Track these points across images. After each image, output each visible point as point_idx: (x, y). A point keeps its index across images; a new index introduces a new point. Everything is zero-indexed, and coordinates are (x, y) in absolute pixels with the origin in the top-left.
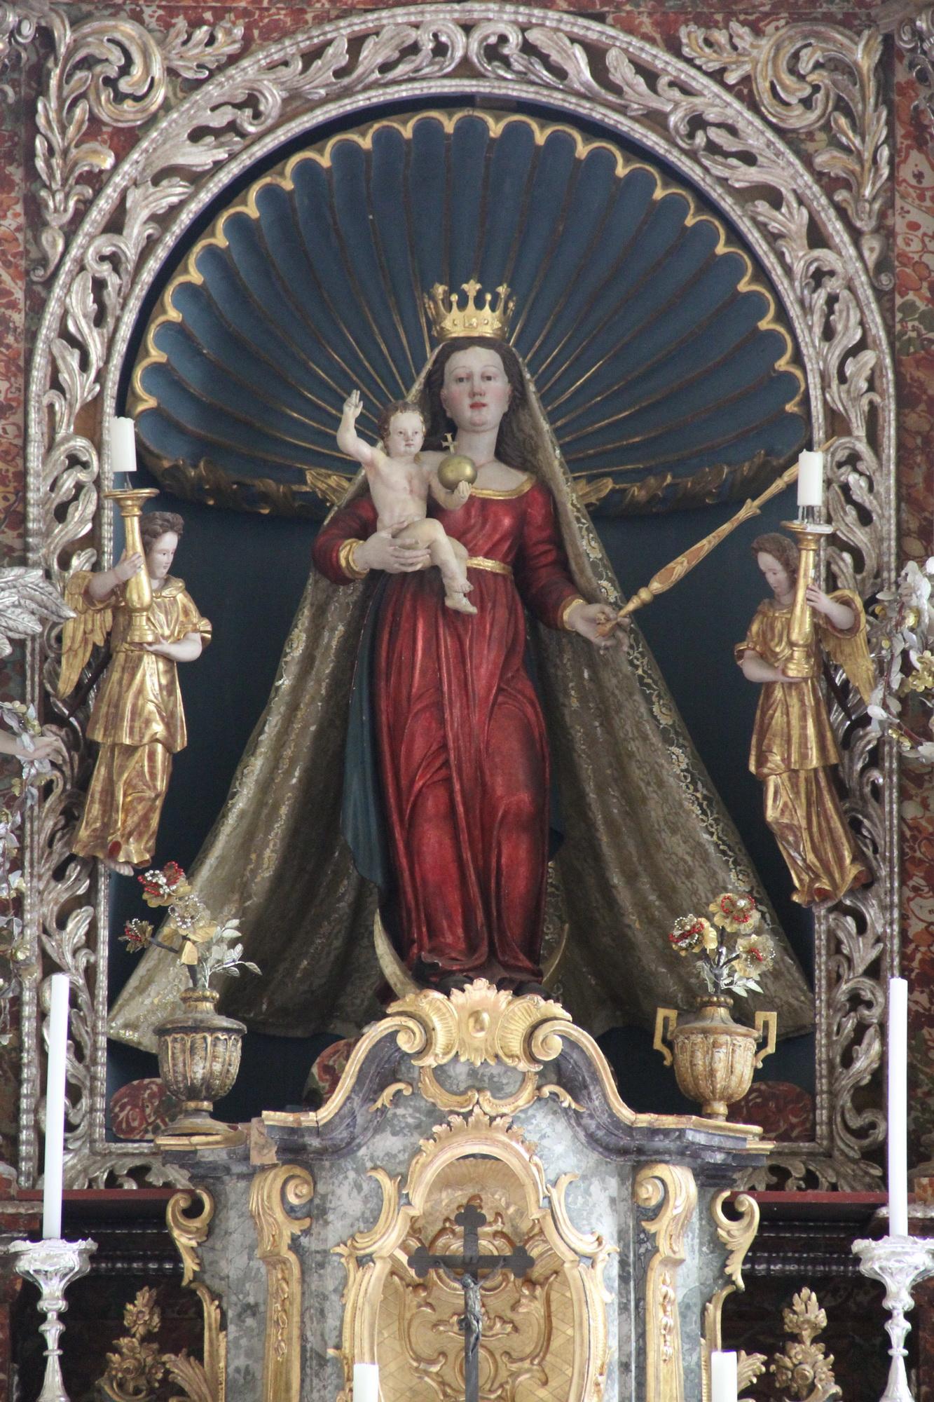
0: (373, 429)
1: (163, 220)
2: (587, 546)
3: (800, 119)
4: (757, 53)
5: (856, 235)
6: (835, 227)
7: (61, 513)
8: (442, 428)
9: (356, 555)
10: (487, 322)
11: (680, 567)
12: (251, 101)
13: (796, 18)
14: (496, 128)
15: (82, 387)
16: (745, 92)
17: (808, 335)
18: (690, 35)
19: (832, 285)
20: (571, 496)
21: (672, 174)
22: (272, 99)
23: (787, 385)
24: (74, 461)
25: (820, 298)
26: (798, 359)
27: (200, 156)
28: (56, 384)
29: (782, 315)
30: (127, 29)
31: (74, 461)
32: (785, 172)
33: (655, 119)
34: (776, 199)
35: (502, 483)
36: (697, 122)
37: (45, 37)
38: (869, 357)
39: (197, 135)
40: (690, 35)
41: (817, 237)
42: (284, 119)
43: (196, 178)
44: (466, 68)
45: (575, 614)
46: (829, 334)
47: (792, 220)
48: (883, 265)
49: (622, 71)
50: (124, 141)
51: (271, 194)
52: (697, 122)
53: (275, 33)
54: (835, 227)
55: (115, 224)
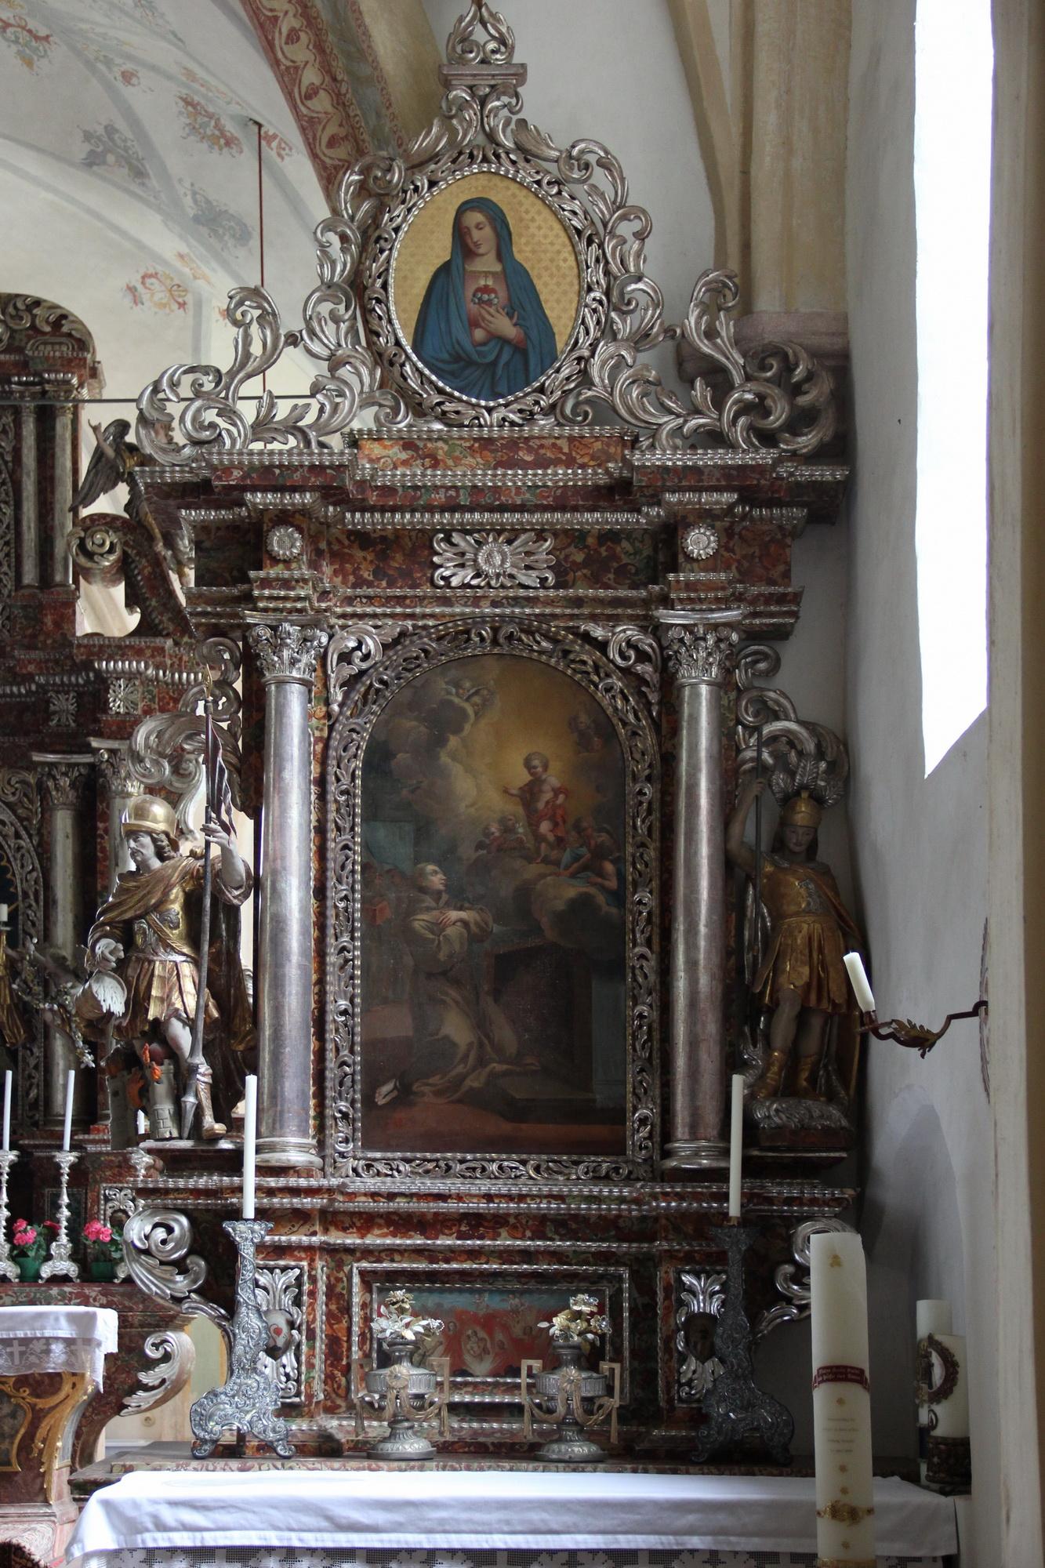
3: (12, 799)
5: (30, 836)
6: (23, 833)
13: (11, 767)
17: (16, 866)
19: (23, 851)
23: (11, 883)
25: (19, 856)
26: (14, 875)
29: (9, 861)
38: (35, 874)
41: (18, 836)
46: (22, 866)
47: (11, 831)
48: (40, 844)
54: (23, 833)
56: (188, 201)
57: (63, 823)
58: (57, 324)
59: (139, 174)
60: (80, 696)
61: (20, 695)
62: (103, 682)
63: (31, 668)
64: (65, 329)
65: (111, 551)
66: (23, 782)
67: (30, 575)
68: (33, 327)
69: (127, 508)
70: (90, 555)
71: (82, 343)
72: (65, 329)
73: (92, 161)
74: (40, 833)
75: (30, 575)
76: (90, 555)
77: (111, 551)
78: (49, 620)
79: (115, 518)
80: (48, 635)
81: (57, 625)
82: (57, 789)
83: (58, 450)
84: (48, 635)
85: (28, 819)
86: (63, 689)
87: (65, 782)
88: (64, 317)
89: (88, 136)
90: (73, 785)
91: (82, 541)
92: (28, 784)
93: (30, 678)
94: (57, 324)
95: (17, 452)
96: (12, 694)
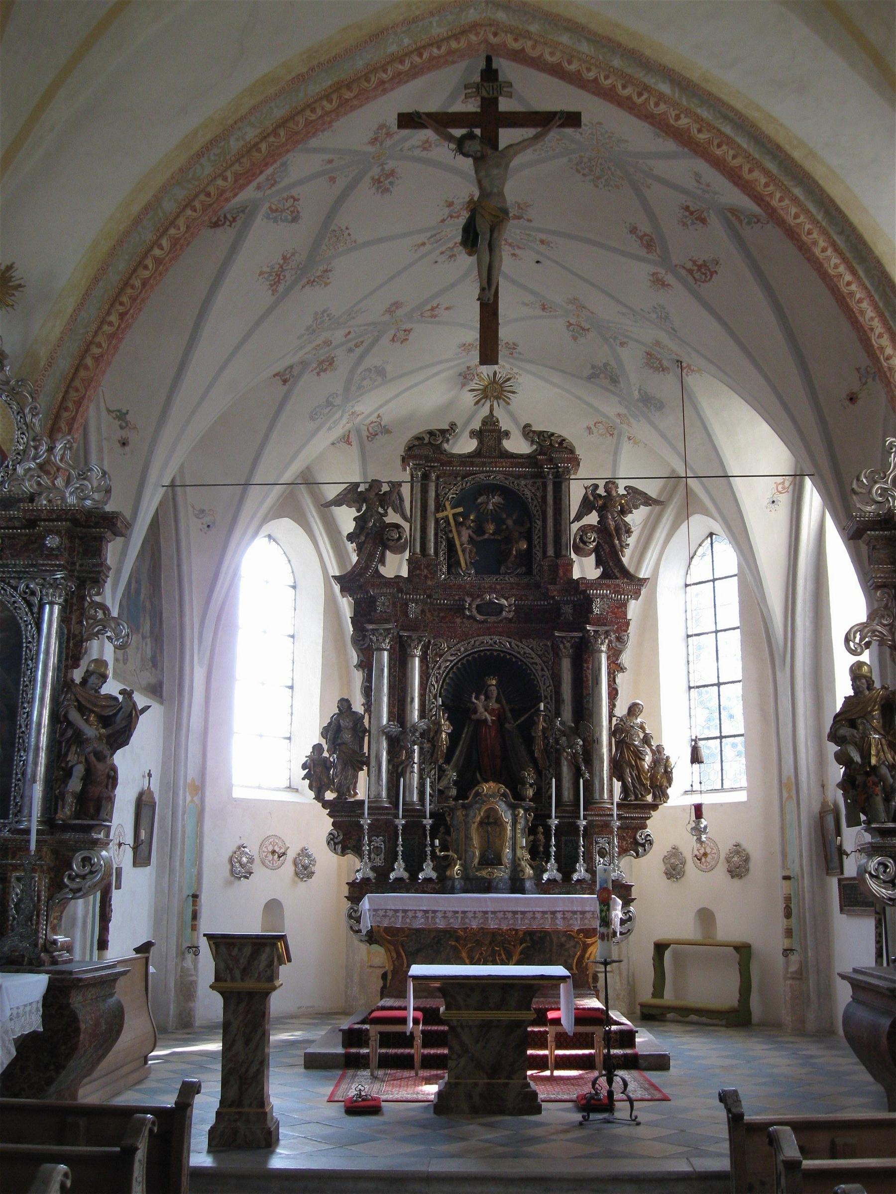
0: (476, 698)
1: (446, 667)
2: (509, 715)
4: (534, 643)
6: (545, 669)
7: (431, 710)
8: (487, 698)
9: (474, 717)
10: (494, 682)
11: (523, 719)
12: (459, 650)
14: (495, 654)
15: (434, 692)
16: (532, 649)
18: (524, 641)
20: (507, 708)
21: (521, 661)
22: (462, 649)
24: (433, 703)
27: (452, 658)
28: (430, 691)
30: (441, 640)
31: (433, 703)
32: (538, 661)
33: (519, 653)
34: (536, 664)
35: (496, 706)
36: (525, 653)
37: (429, 641)
39: (452, 655)
40: (524, 641)
41: (543, 670)
42: (465, 652)
43: (451, 661)
44: (491, 645)
45: (507, 726)
49: (513, 645)
50: (441, 656)
51: (462, 664)
52: (525, 653)
53: (463, 640)
54: (545, 669)
55: (439, 668)
56: (636, 393)
57: (566, 665)
58: (561, 443)
59: (615, 381)
60: (574, 606)
61: (544, 605)
62: (589, 601)
63: (555, 593)
64: (564, 445)
65: (594, 541)
66: (546, 645)
67: (551, 552)
68: (551, 444)
69: (599, 522)
70: (585, 543)
71: (572, 451)
72: (564, 445)
73: (592, 377)
74: (552, 669)
75: (551, 552)
76: (585, 543)
77: (594, 541)
78: (561, 572)
79: (595, 526)
80: (561, 579)
81: (565, 574)
82: (565, 647)
83: (563, 496)
84: (561, 579)
85: (547, 662)
86: (567, 603)
87: (568, 645)
88: (564, 440)
89: (593, 367)
90: (572, 647)
91: (581, 536)
92: (546, 645)
93: (553, 597)
94: (561, 443)
95: (544, 498)
96: (541, 605)
